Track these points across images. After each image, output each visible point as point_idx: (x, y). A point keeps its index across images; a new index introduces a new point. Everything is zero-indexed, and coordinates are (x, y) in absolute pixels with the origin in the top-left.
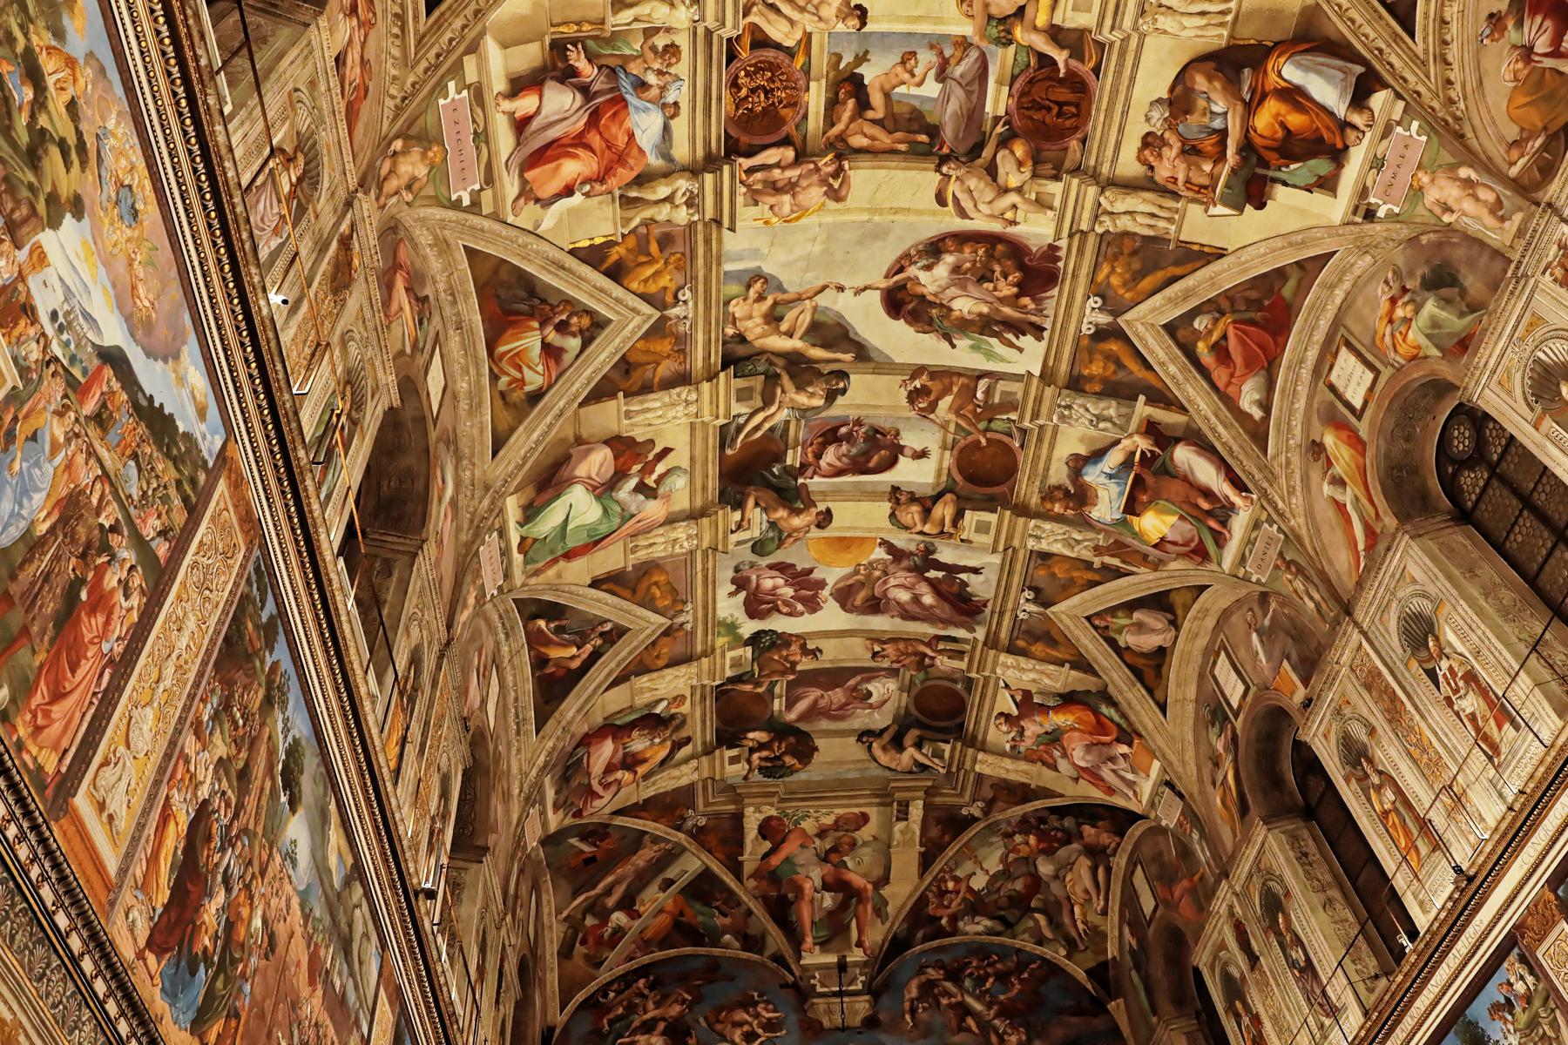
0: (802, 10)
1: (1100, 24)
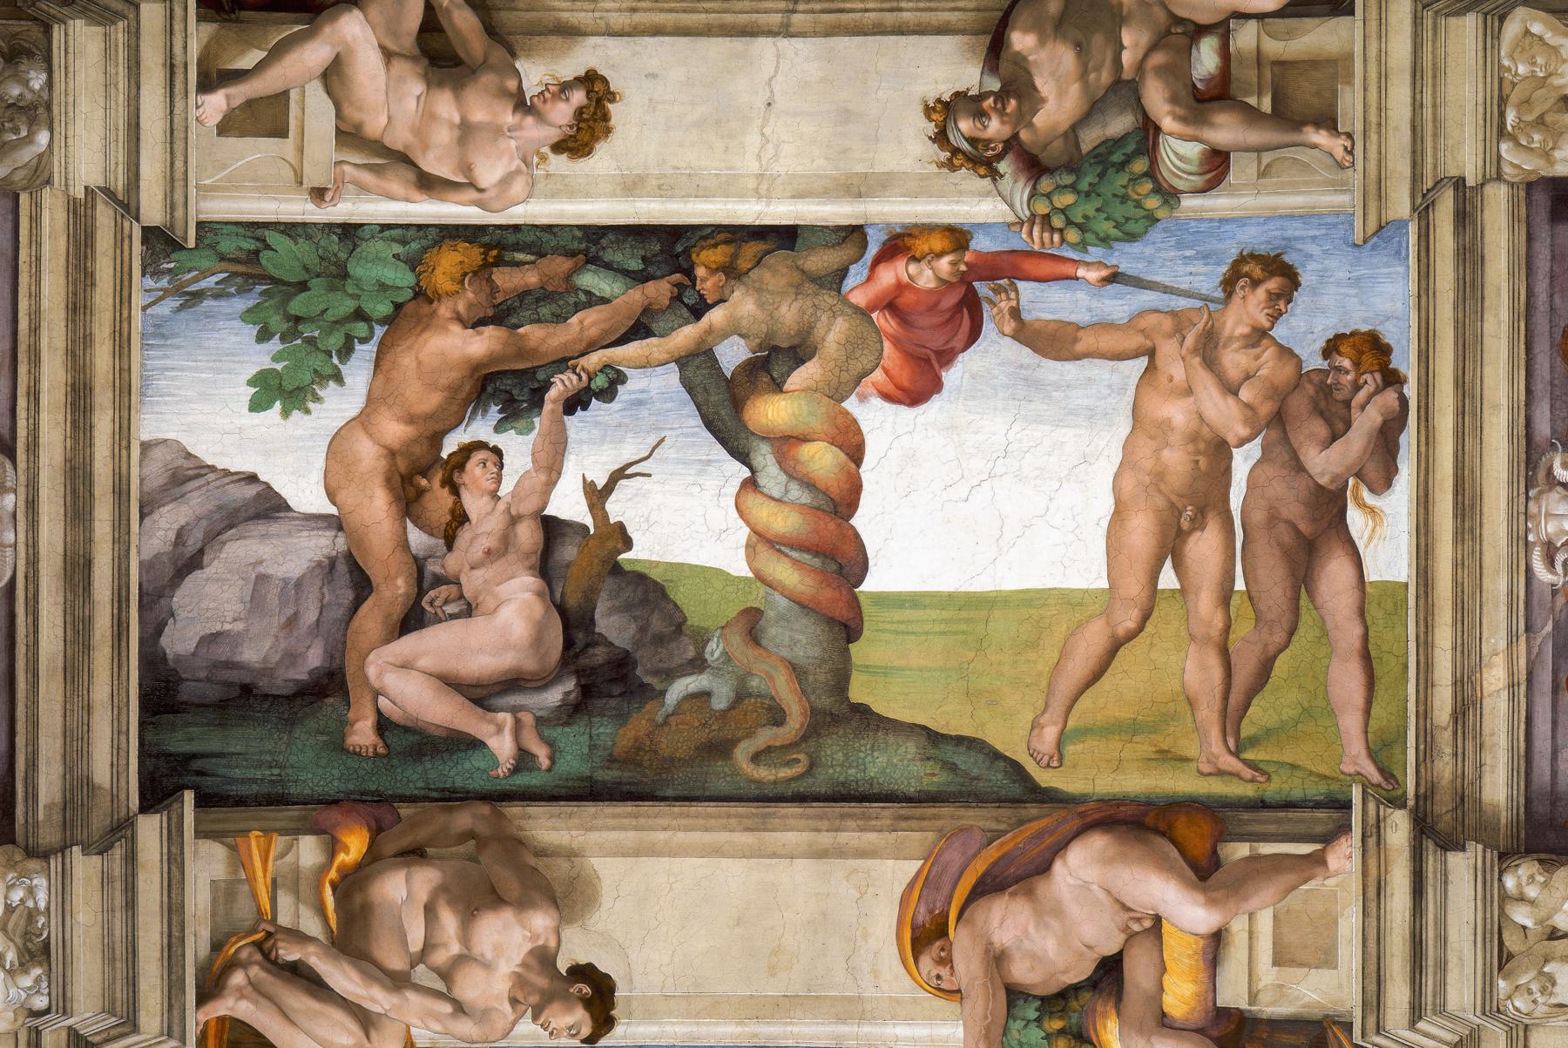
0: (398, 981)
1: (1374, 1001)
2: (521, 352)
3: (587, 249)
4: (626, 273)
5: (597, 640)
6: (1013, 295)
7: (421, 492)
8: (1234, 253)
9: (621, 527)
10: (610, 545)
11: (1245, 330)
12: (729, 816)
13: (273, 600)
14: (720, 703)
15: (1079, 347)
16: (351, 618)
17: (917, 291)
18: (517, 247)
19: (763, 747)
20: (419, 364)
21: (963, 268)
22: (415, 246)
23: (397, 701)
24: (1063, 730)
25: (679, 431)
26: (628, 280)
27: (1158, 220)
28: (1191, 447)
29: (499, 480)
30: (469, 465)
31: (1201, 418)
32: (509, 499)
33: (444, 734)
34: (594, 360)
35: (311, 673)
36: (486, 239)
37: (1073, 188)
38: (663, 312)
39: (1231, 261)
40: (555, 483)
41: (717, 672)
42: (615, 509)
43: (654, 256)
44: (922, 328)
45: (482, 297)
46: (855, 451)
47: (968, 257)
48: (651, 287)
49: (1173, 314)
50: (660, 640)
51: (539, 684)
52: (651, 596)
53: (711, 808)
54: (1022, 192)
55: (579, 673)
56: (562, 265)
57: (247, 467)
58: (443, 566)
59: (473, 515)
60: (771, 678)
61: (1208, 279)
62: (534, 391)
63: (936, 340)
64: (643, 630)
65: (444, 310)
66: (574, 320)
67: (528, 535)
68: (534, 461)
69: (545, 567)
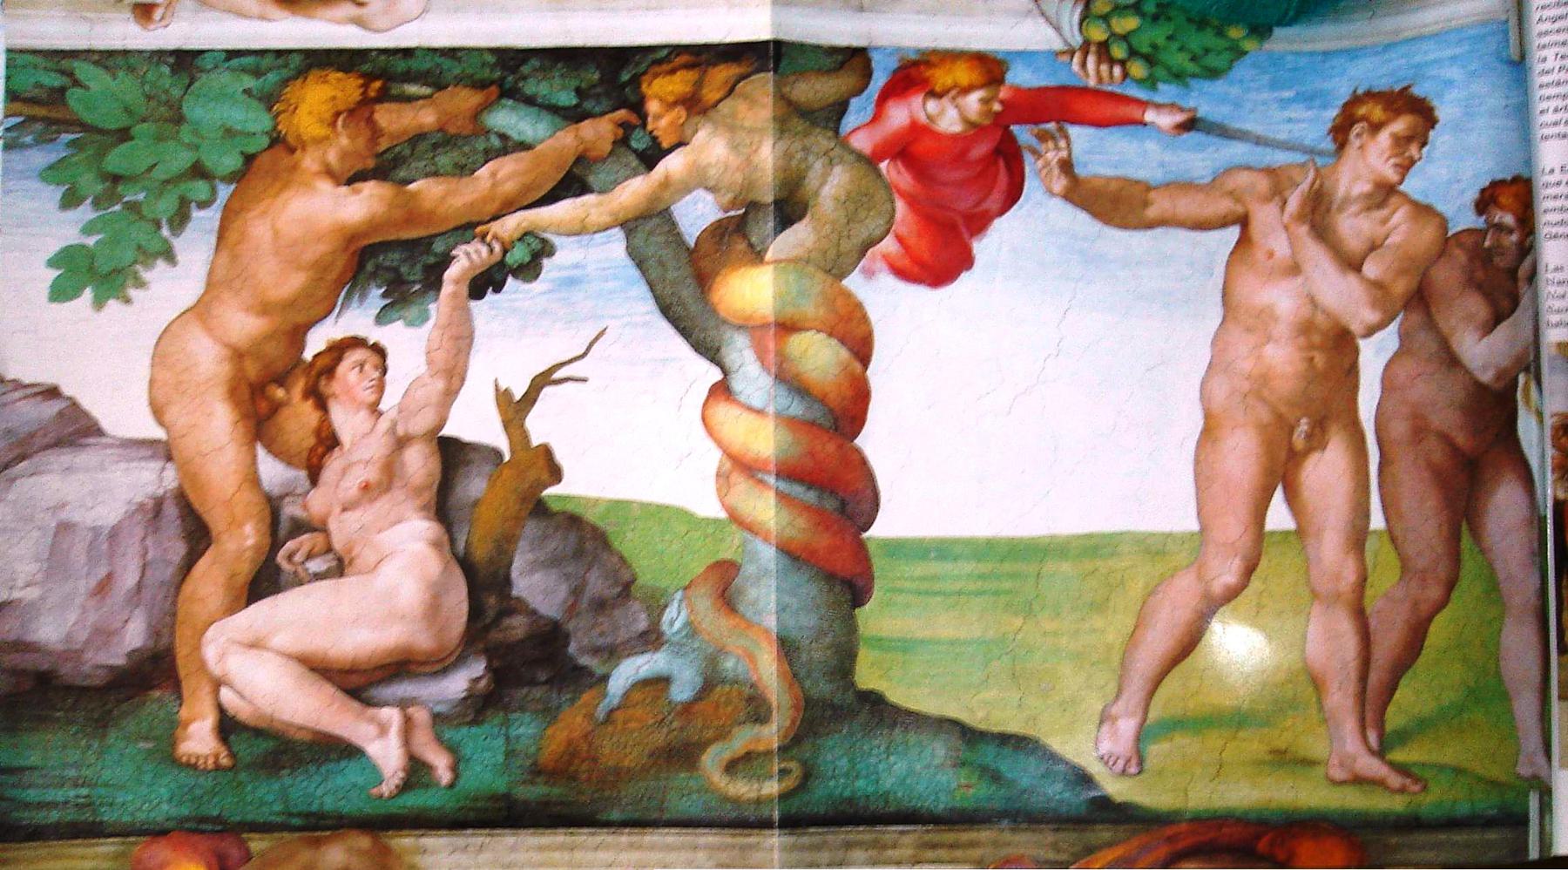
2: (412, 216)
3: (501, 81)
4: (553, 109)
5: (512, 606)
6: (1062, 144)
7: (276, 407)
8: (1343, 93)
9: (546, 452)
10: (532, 475)
11: (1363, 187)
12: (695, 848)
13: (78, 554)
14: (682, 692)
15: (1152, 213)
16: (183, 580)
17: (938, 136)
18: (409, 77)
19: (743, 752)
20: (276, 234)
21: (997, 107)
22: (272, 77)
23: (247, 693)
24: (1144, 720)
25: (625, 320)
26: (557, 120)
27: (1246, 53)
28: (1302, 340)
29: (380, 388)
30: (342, 368)
31: (1313, 301)
32: (393, 414)
33: (307, 737)
34: (511, 224)
35: (131, 654)
36: (366, 67)
37: (1136, 8)
38: (604, 160)
39: (1341, 102)
40: (457, 392)
41: (679, 650)
42: (540, 426)
43: (594, 86)
44: (945, 184)
45: (361, 142)
46: (861, 348)
47: (1003, 93)
48: (588, 129)
49: (1270, 171)
50: (600, 606)
51: (438, 667)
52: (589, 545)
53: (671, 837)
54: (1072, 11)
55: (491, 653)
56: (466, 99)
57: (46, 377)
58: (305, 507)
59: (345, 436)
60: (752, 658)
61: (1313, 126)
62: (428, 269)
63: (965, 202)
64: (577, 592)
65: (309, 161)
66: (484, 172)
67: (419, 463)
68: (430, 362)
69: (443, 508)
